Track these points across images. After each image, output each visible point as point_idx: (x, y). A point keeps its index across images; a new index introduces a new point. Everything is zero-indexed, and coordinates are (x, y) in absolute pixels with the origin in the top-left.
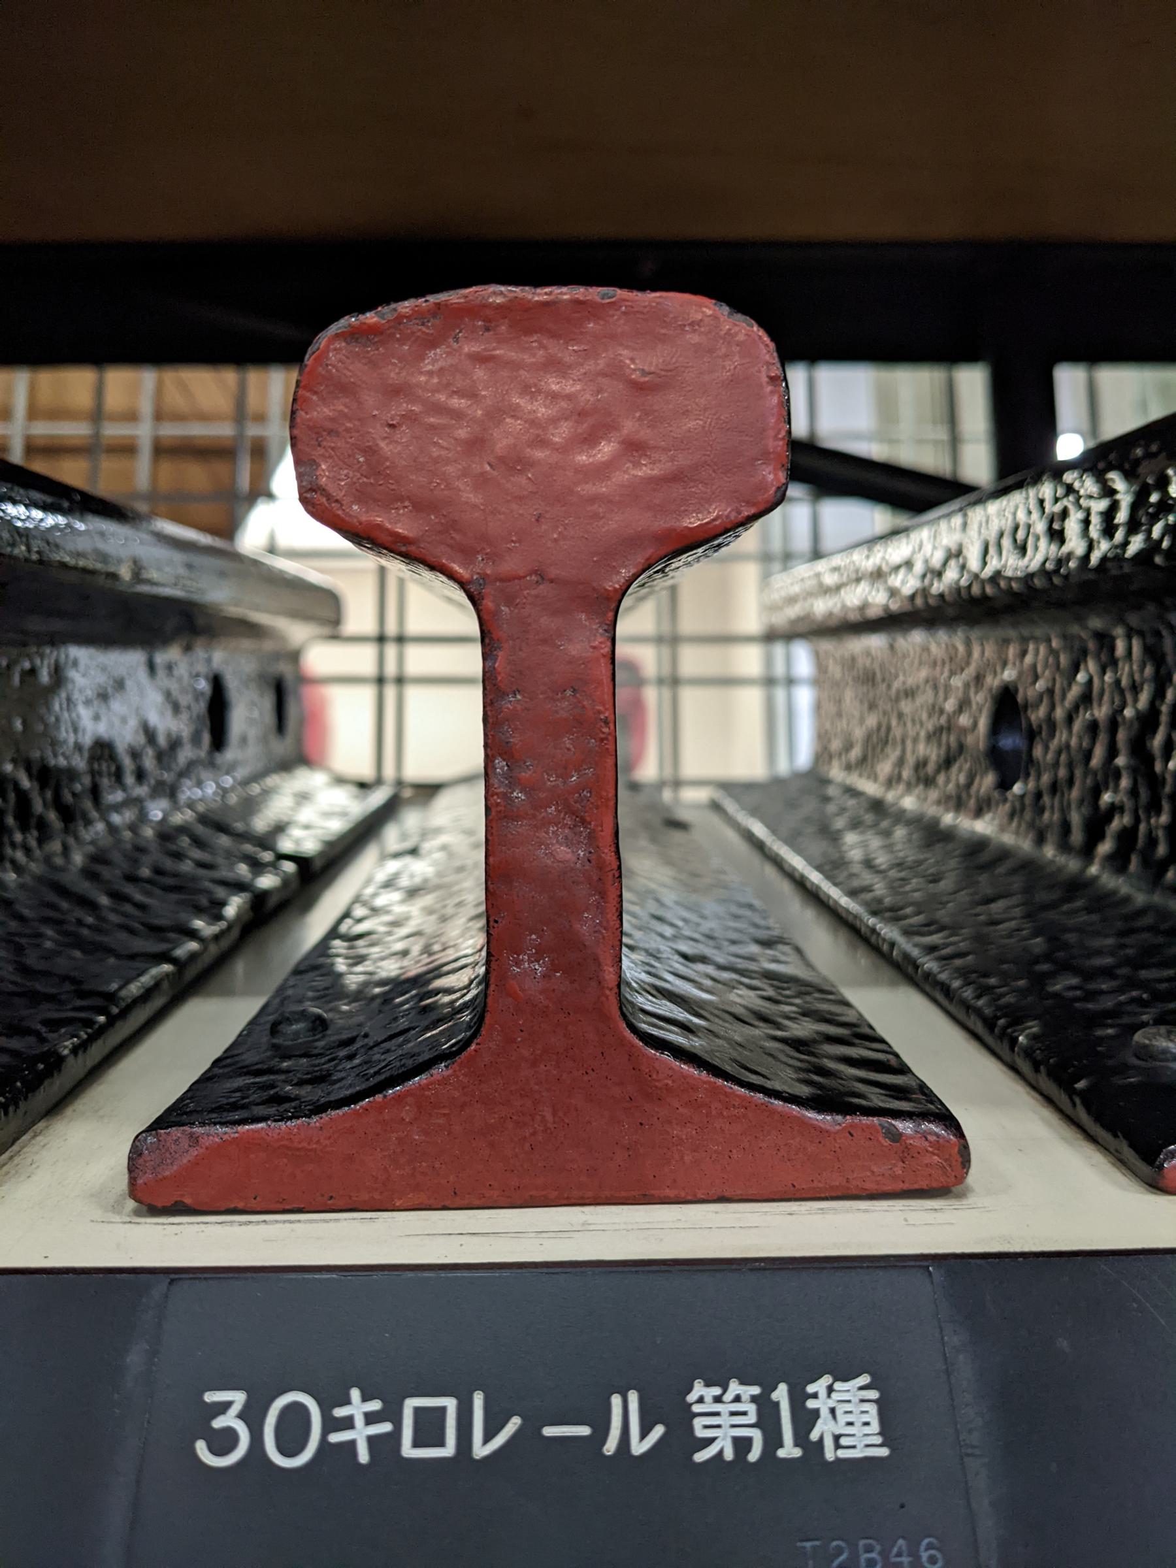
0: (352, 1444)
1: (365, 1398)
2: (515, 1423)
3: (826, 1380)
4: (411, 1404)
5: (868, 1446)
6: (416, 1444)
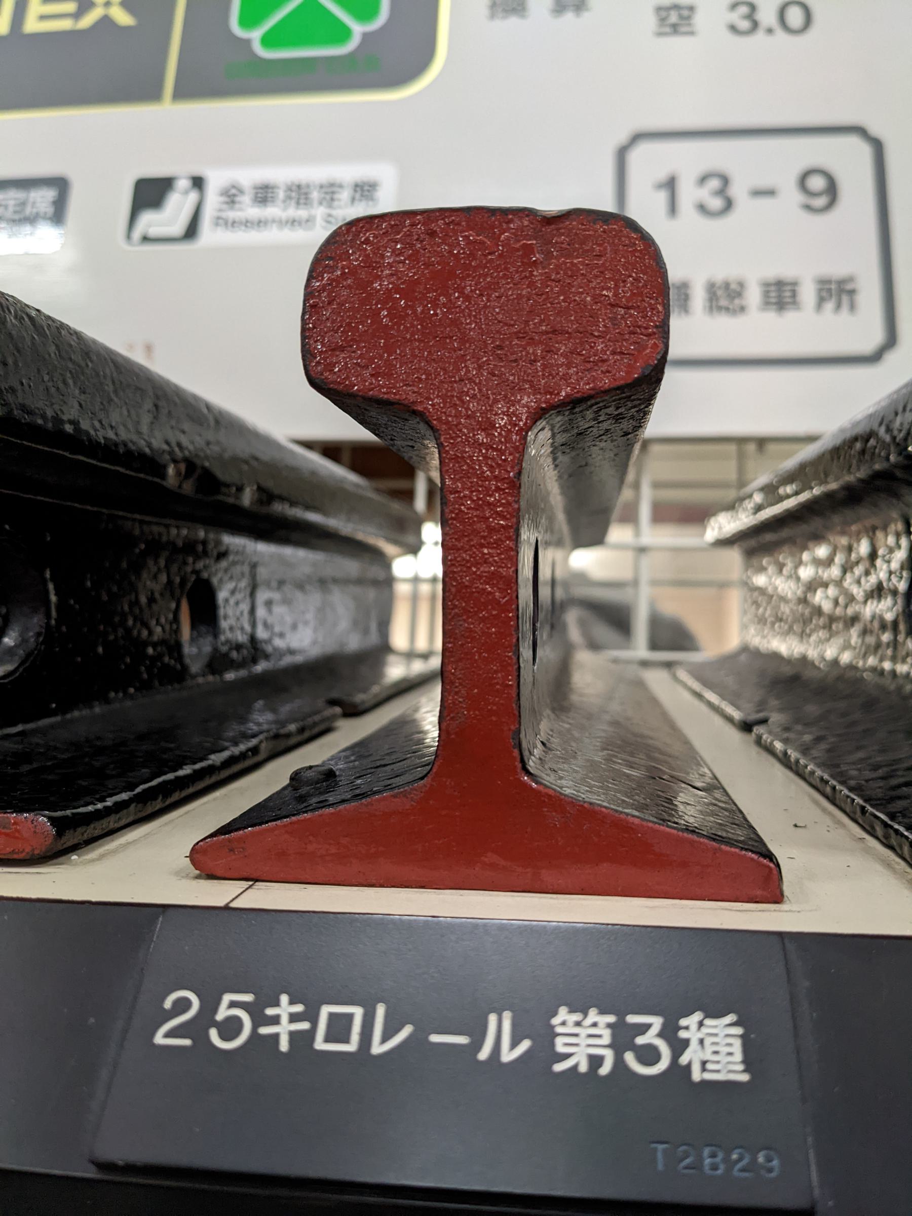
0: (276, 1037)
1: (292, 1002)
2: (406, 1032)
3: (697, 1016)
4: (326, 1010)
5: (730, 1071)
6: (327, 1040)
